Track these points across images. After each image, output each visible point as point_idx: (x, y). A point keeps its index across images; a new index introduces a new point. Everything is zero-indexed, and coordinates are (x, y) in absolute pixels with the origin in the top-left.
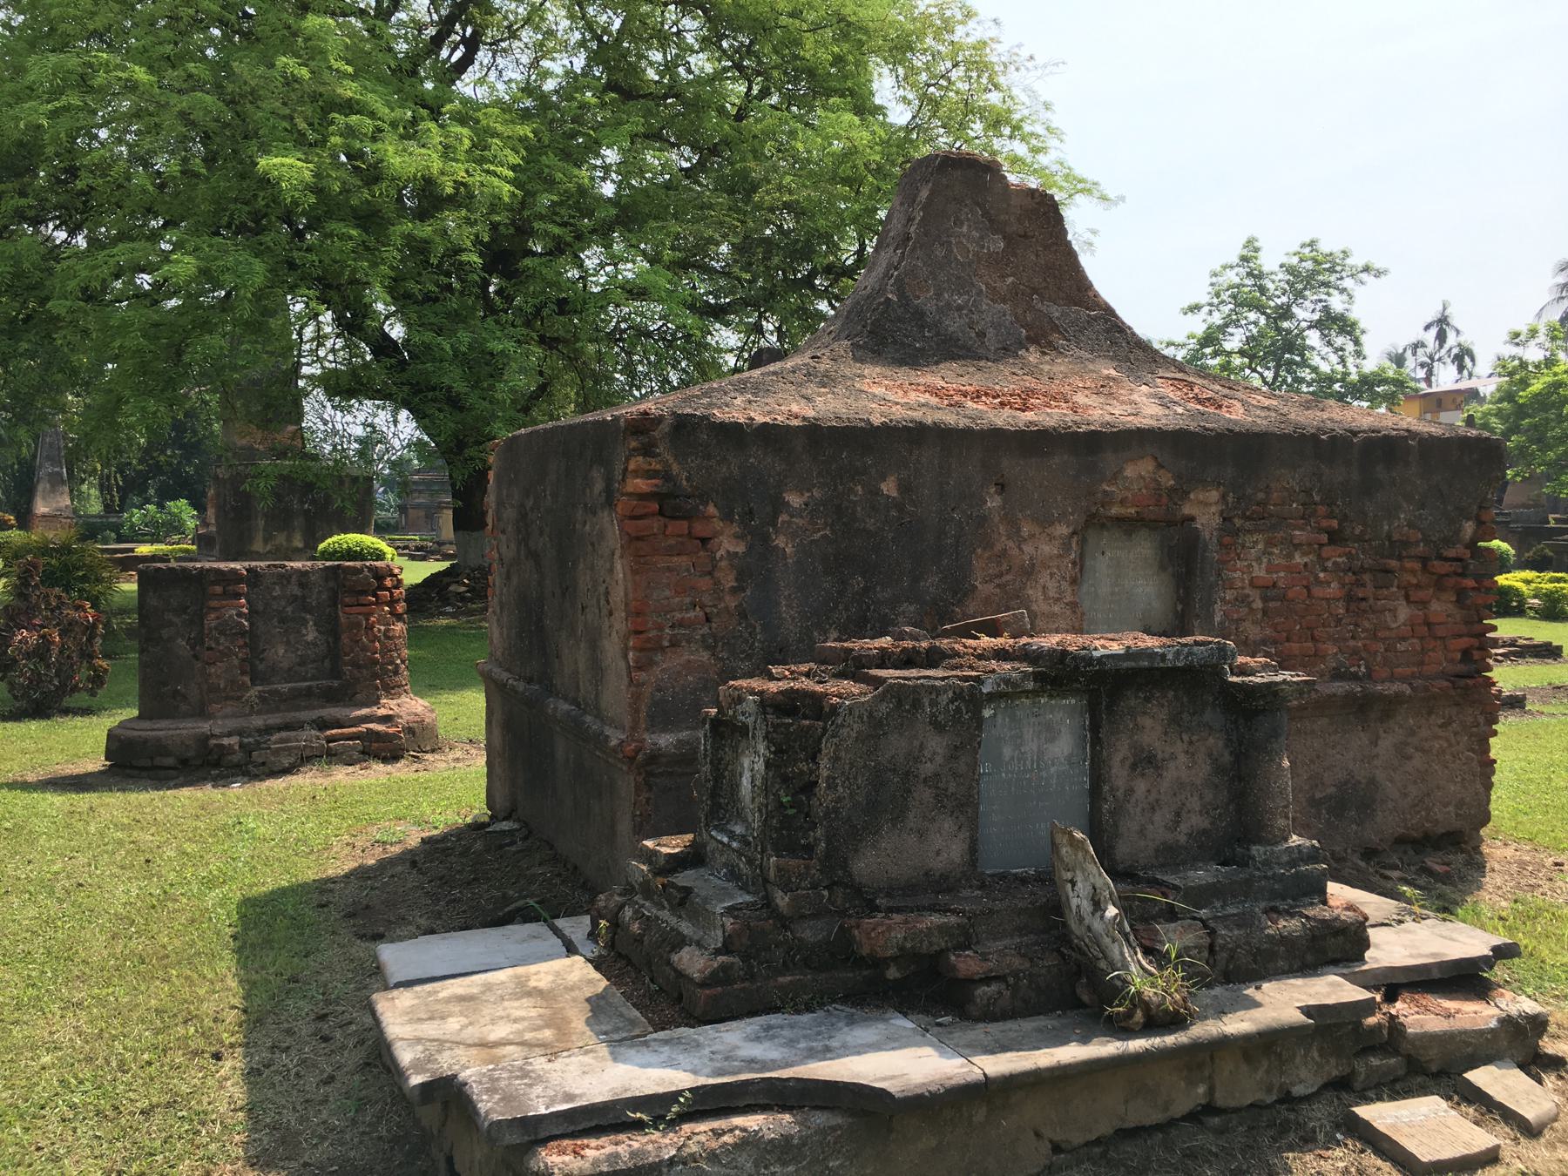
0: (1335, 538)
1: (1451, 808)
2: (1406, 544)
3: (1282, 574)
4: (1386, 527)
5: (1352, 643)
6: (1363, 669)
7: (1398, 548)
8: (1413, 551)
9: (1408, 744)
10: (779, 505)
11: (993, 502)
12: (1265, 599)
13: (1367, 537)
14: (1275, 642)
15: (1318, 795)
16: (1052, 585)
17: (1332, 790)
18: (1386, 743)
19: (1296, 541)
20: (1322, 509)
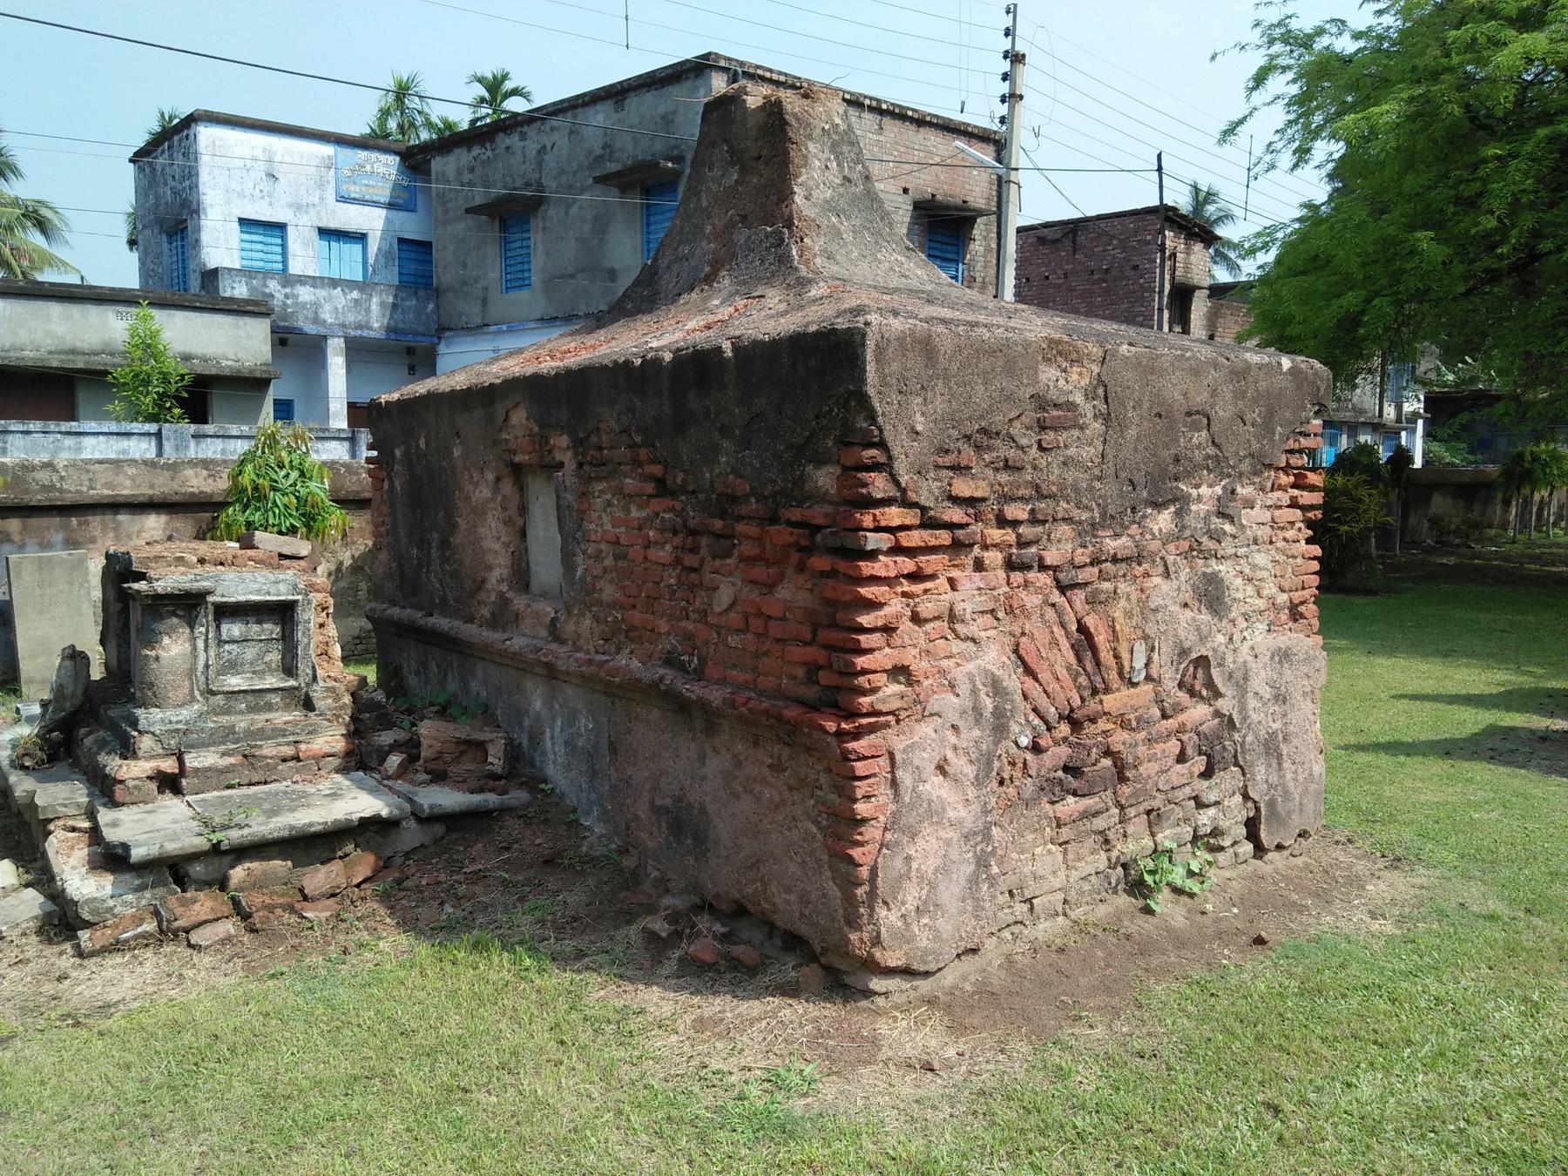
0: (663, 488)
1: (792, 897)
2: (734, 499)
3: (623, 529)
4: (708, 475)
5: (684, 624)
6: (696, 661)
7: (726, 504)
8: (743, 510)
9: (736, 778)
10: (394, 456)
11: (457, 452)
12: (616, 558)
13: (691, 488)
14: (622, 608)
15: (659, 802)
16: (493, 525)
17: (668, 802)
18: (714, 765)
19: (626, 491)
20: (643, 452)
